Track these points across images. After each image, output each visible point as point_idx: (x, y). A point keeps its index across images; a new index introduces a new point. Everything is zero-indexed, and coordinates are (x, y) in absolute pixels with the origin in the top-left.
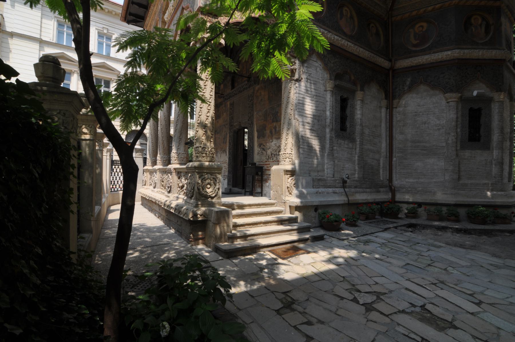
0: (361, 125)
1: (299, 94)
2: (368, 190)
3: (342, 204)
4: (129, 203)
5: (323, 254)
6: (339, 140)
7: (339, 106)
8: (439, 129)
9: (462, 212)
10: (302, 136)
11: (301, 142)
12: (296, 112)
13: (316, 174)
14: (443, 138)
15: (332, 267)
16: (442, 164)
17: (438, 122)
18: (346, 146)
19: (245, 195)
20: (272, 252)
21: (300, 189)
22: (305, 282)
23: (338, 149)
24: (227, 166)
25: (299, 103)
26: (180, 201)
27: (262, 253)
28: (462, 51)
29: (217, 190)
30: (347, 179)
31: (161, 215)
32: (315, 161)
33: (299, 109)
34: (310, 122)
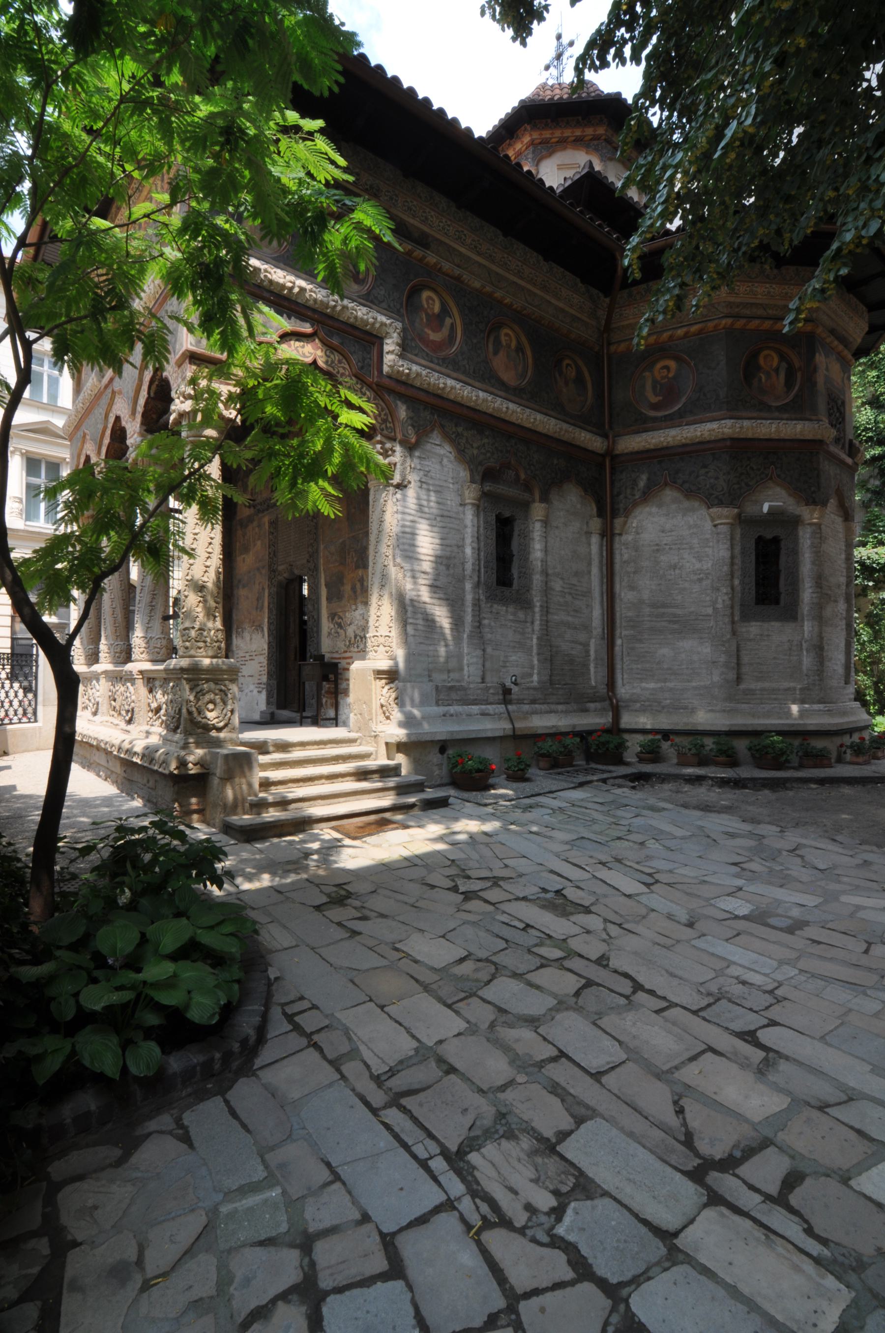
0: (545, 573)
1: (404, 513)
2: (560, 707)
3: (501, 738)
4: (67, 729)
5: (435, 829)
6: (495, 606)
7: (493, 535)
9: (741, 745)
10: (412, 600)
11: (407, 609)
12: (397, 551)
13: (445, 677)
14: (708, 598)
15: (440, 846)
16: (706, 650)
17: (698, 565)
18: (511, 617)
21: (408, 708)
22: (384, 874)
23: (493, 624)
25: (404, 532)
26: (154, 740)
27: (316, 831)
28: (739, 423)
29: (229, 714)
30: (512, 686)
31: (112, 772)
32: (442, 651)
33: (404, 544)
34: (429, 570)
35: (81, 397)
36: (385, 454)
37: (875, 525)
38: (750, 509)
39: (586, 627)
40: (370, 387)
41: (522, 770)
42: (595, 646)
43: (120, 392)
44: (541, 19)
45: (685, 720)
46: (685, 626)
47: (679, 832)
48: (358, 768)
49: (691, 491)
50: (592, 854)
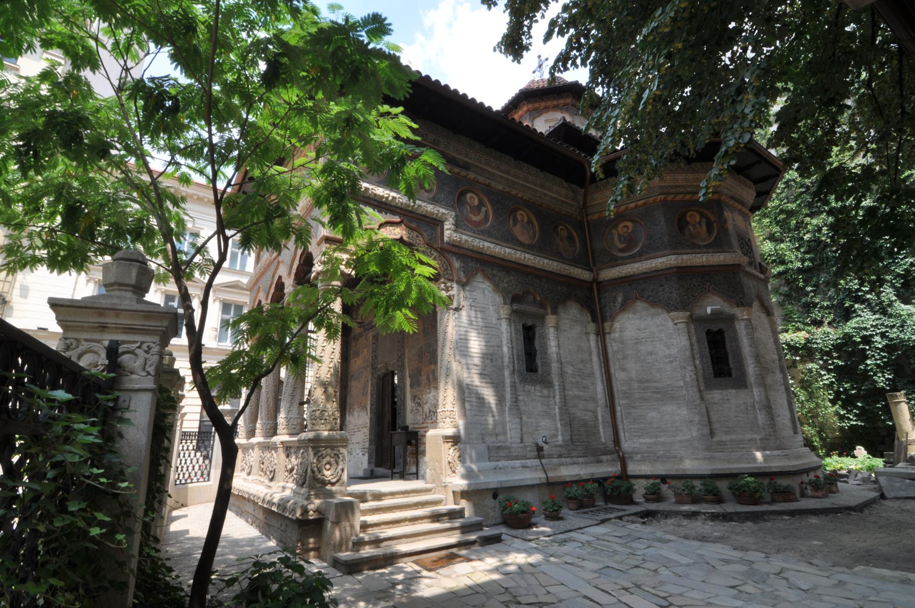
0: (560, 361)
2: (580, 460)
4: (226, 486)
5: (491, 562)
8: (671, 362)
9: (723, 486)
10: (468, 385)
11: (465, 392)
12: (457, 352)
13: (494, 439)
15: (495, 577)
16: (684, 412)
17: (668, 352)
19: (392, 477)
20: (415, 562)
21: (468, 464)
24: (368, 433)
26: (288, 493)
27: (400, 565)
28: (680, 257)
34: (479, 363)
35: (259, 266)
36: (447, 290)
37: (791, 317)
38: (698, 312)
39: (593, 399)
40: (436, 250)
41: (556, 511)
42: (601, 413)
43: (283, 262)
44: (527, 49)
45: (676, 467)
46: (665, 395)
47: (684, 560)
48: (433, 512)
49: (655, 302)
50: (617, 581)
